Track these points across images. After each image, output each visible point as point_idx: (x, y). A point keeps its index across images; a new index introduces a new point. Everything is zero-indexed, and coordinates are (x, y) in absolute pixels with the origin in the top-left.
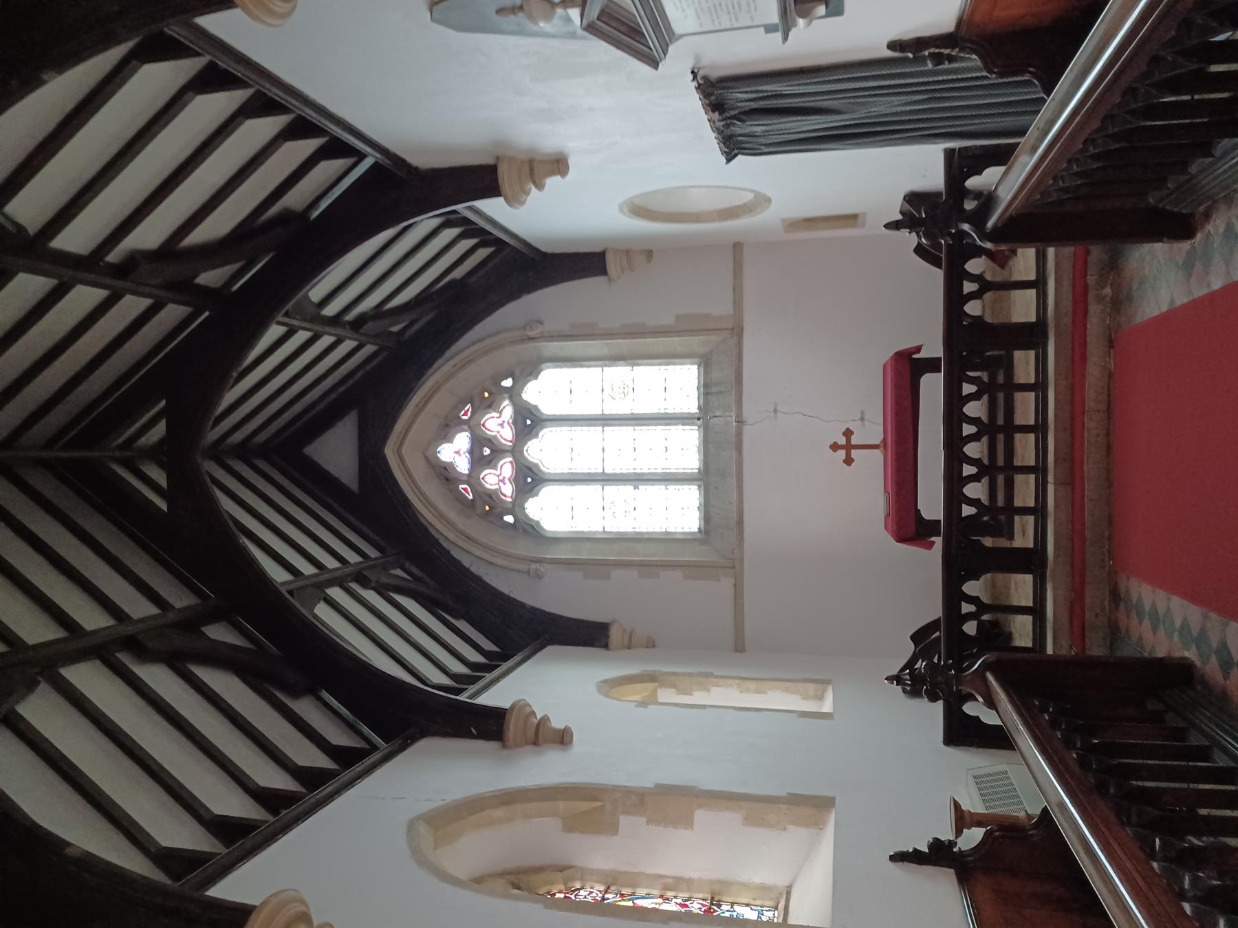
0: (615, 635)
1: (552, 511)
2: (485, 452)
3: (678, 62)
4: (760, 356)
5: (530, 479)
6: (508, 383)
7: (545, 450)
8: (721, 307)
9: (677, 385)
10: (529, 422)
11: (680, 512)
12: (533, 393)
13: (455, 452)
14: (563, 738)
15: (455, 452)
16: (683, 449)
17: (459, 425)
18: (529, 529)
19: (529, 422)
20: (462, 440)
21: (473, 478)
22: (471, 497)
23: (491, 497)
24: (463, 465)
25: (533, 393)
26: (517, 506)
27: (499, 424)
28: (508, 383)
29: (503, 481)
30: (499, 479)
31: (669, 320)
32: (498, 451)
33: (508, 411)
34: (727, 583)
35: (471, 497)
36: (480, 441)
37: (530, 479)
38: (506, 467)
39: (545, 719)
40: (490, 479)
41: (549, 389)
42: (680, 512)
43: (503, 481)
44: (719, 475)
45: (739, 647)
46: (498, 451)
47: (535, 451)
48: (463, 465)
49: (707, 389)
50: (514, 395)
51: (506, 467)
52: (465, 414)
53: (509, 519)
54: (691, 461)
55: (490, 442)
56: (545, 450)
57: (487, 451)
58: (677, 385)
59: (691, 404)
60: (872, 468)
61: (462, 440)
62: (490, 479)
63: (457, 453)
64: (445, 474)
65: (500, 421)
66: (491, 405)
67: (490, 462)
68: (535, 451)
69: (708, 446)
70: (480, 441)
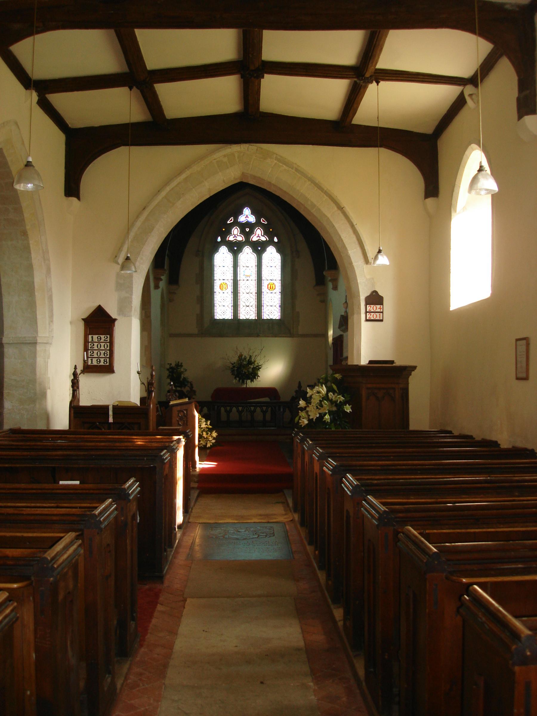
1: (222, 258)
2: (247, 229)
3: (342, 333)
5: (235, 249)
6: (276, 240)
7: (247, 255)
9: (272, 310)
10: (259, 249)
11: (222, 310)
13: (247, 216)
15: (247, 216)
16: (247, 313)
18: (215, 248)
19: (259, 249)
20: (252, 219)
22: (228, 222)
23: (229, 232)
24: (242, 219)
27: (258, 235)
28: (276, 240)
29: (235, 237)
30: (236, 235)
32: (247, 235)
34: (196, 331)
35: (228, 222)
37: (235, 249)
39: (161, 280)
40: (236, 231)
41: (272, 258)
42: (222, 310)
43: (235, 237)
44: (237, 327)
46: (247, 235)
48: (242, 219)
50: (270, 242)
52: (263, 221)
53: (219, 239)
54: (242, 316)
55: (252, 232)
56: (247, 255)
57: (247, 230)
59: (265, 316)
61: (252, 219)
62: (236, 231)
63: (247, 216)
65: (260, 235)
67: (243, 232)
69: (248, 322)
70: (252, 226)
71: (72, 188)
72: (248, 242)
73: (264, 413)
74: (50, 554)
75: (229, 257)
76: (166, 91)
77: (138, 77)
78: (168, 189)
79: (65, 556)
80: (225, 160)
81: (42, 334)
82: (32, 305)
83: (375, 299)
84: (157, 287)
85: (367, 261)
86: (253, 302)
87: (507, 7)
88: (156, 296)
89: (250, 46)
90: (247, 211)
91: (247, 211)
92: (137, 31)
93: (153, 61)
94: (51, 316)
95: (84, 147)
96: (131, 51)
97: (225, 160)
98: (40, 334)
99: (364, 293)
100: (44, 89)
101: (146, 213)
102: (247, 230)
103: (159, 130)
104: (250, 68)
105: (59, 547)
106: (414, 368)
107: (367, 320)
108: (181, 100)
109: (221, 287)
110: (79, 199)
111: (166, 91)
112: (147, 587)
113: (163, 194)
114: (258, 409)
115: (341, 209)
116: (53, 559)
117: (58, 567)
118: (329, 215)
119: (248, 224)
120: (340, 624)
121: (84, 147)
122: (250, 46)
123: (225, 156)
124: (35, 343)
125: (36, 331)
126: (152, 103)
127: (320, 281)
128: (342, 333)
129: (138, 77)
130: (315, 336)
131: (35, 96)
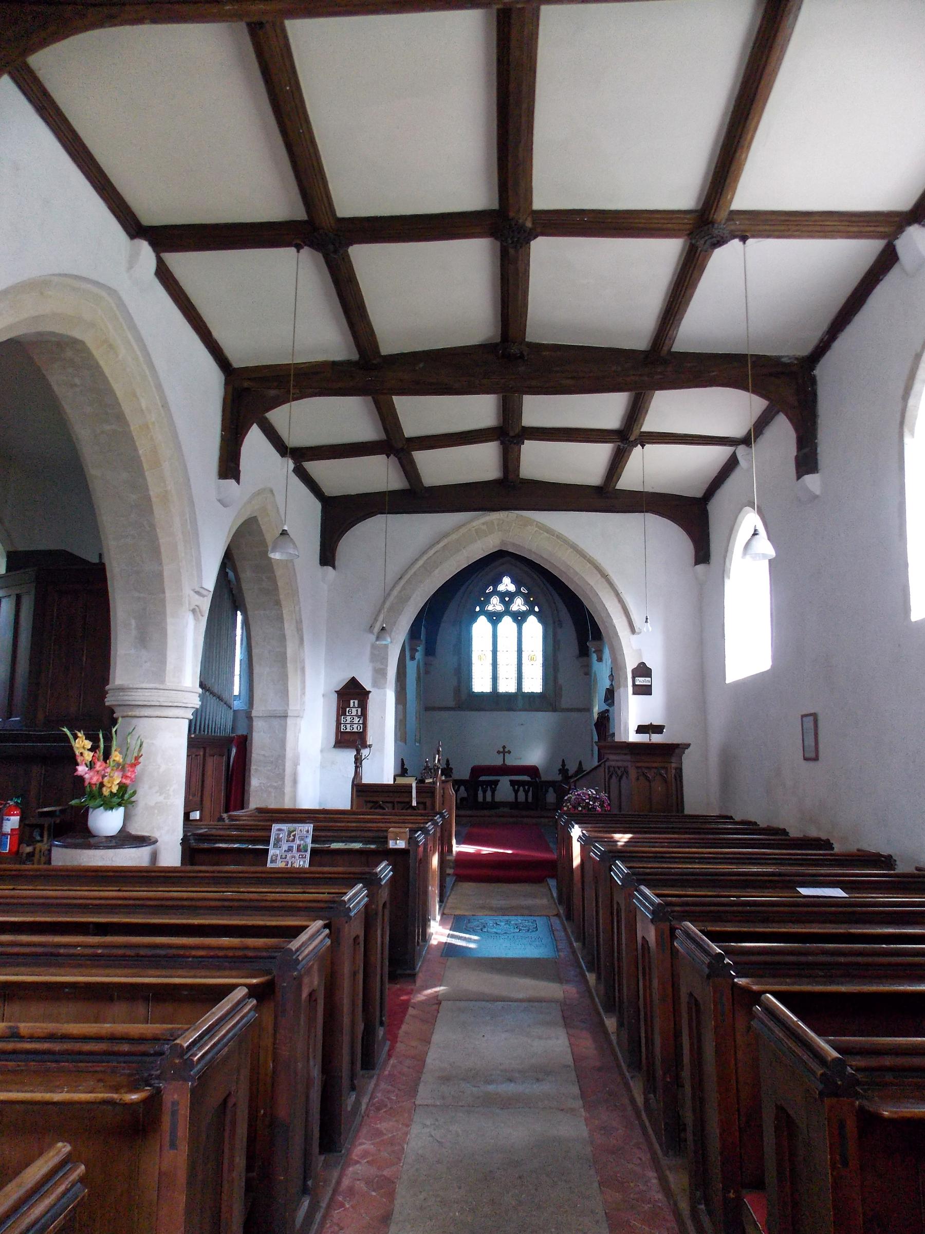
0: (430, 658)
1: (481, 628)
3: (607, 707)
4: (543, 720)
5: (495, 618)
6: (537, 609)
7: (507, 625)
8: (564, 704)
9: (534, 683)
11: (481, 684)
12: (532, 621)
13: (507, 585)
14: (413, 658)
15: (507, 585)
16: (507, 686)
17: (518, 589)
18: (474, 617)
20: (512, 588)
21: (495, 592)
23: (487, 602)
24: (501, 588)
25: (532, 621)
26: (483, 612)
27: (519, 605)
30: (495, 604)
31: (561, 681)
32: (507, 604)
33: (524, 608)
34: (451, 703)
36: (512, 596)
37: (495, 618)
38: (500, 608)
39: (417, 651)
40: (495, 600)
41: (534, 628)
42: (481, 684)
44: (496, 701)
45: (427, 709)
46: (507, 604)
47: (507, 621)
48: (501, 588)
49: (532, 695)
50: (531, 612)
51: (500, 608)
53: (478, 609)
55: (511, 601)
56: (507, 625)
58: (534, 683)
60: (498, 761)
61: (512, 588)
62: (495, 600)
64: (497, 581)
66: (527, 602)
67: (502, 601)
68: (507, 621)
69: (508, 696)
70: (512, 596)
71: (327, 557)
72: (507, 612)
73: (526, 792)
74: (294, 945)
75: (489, 626)
76: (424, 459)
77: (395, 444)
78: (425, 558)
79: (311, 948)
80: (484, 527)
81: (293, 708)
82: (284, 678)
83: (643, 670)
84: (413, 658)
85: (633, 631)
86: (514, 675)
87: (784, 360)
88: (412, 668)
89: (510, 411)
90: (506, 580)
91: (506, 580)
92: (395, 398)
93: (410, 429)
94: (304, 688)
95: (340, 516)
96: (388, 418)
97: (484, 527)
98: (291, 707)
99: (631, 664)
100: (300, 456)
101: (403, 582)
102: (507, 599)
103: (416, 498)
104: (509, 434)
105: (304, 937)
106: (688, 746)
107: (634, 693)
108: (439, 468)
109: (480, 658)
110: (334, 567)
111: (424, 459)
112: (398, 986)
113: (421, 563)
114: (521, 788)
115: (605, 577)
116: (297, 950)
117: (303, 959)
118: (592, 584)
119: (507, 593)
120: (614, 1038)
121: (340, 516)
122: (510, 411)
123: (483, 524)
124: (286, 717)
125: (288, 705)
126: (410, 470)
127: (584, 652)
128: (607, 707)
129: (395, 444)
130: (579, 710)
131: (291, 465)
